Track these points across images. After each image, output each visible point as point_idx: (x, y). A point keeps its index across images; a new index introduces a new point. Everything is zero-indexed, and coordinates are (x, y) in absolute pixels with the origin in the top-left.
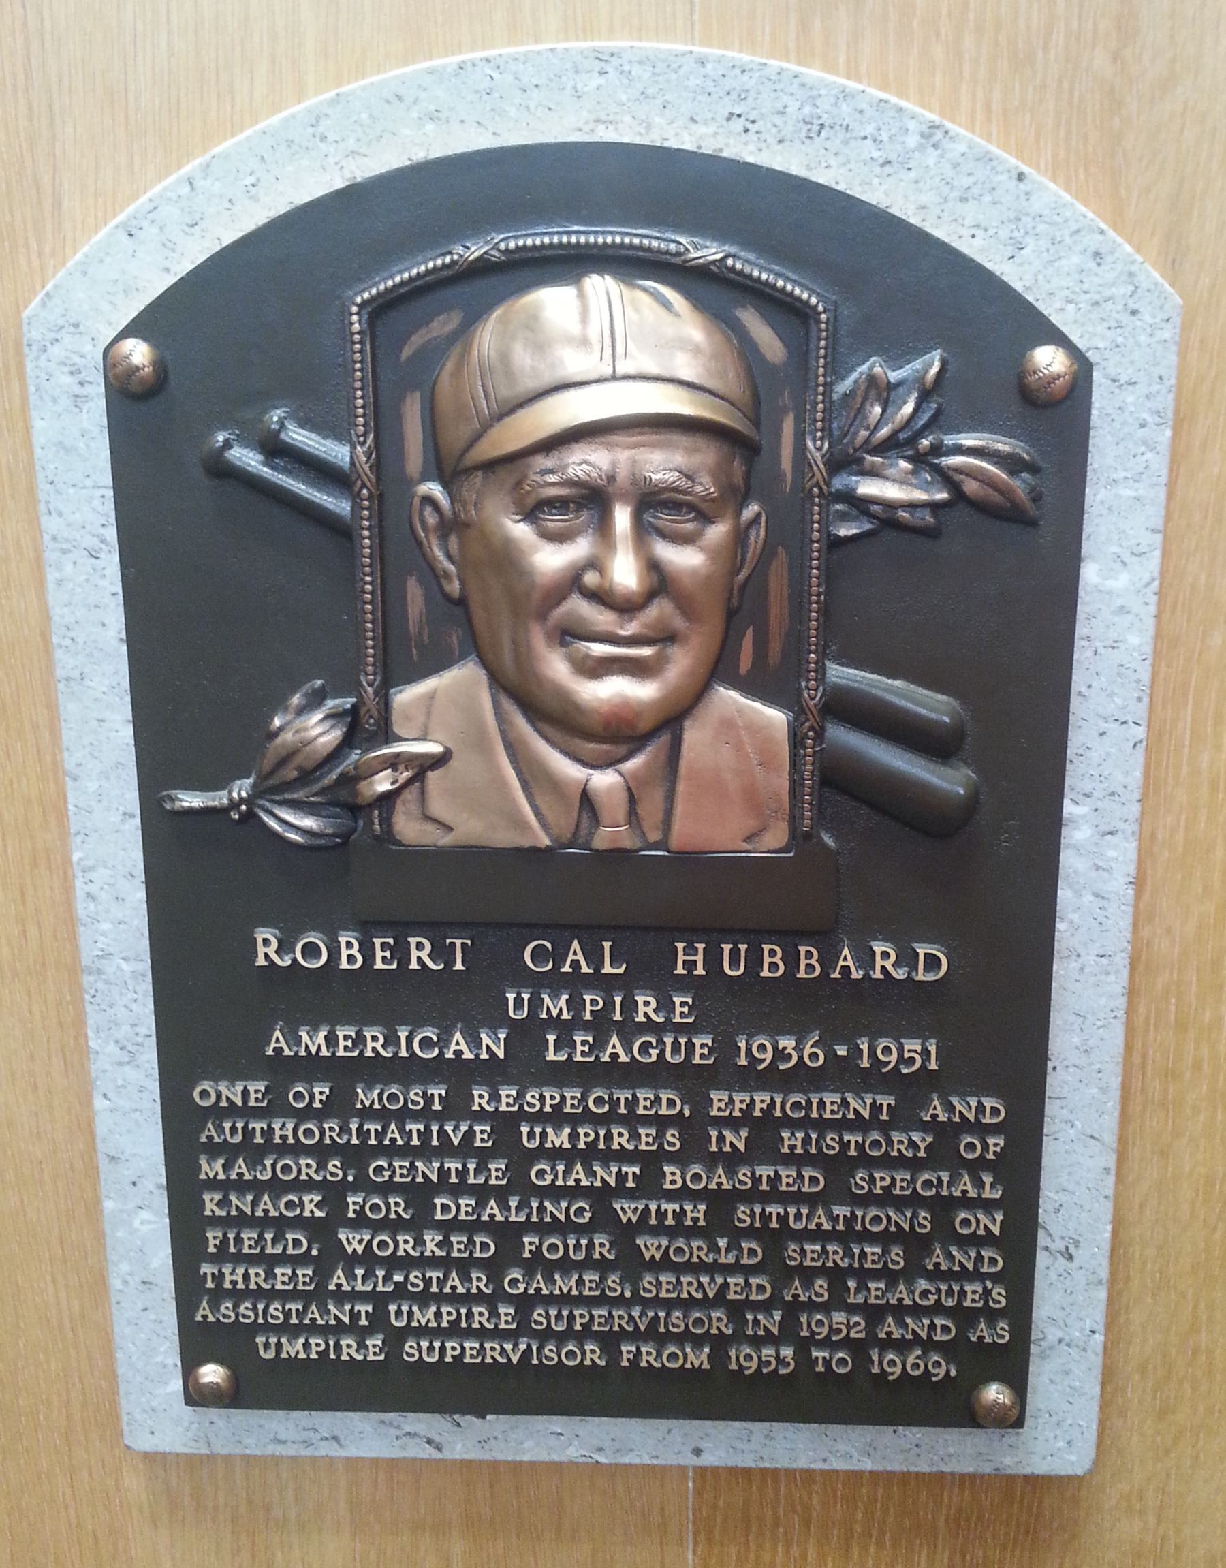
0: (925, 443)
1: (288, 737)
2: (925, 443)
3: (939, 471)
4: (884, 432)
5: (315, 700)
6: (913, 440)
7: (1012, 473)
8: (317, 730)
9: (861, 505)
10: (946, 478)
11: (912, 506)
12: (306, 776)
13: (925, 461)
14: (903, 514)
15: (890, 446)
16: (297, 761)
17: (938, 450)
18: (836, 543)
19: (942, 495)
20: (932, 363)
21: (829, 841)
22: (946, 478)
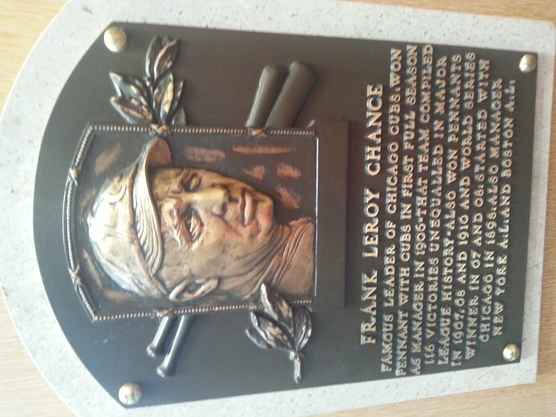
0: (148, 83)
2: (148, 83)
3: (159, 78)
4: (142, 100)
6: (147, 89)
7: (162, 48)
10: (162, 75)
11: (175, 90)
12: (284, 332)
16: (280, 337)
17: (151, 79)
18: (189, 122)
19: (171, 76)
20: (116, 79)
21: (312, 123)
22: (162, 75)
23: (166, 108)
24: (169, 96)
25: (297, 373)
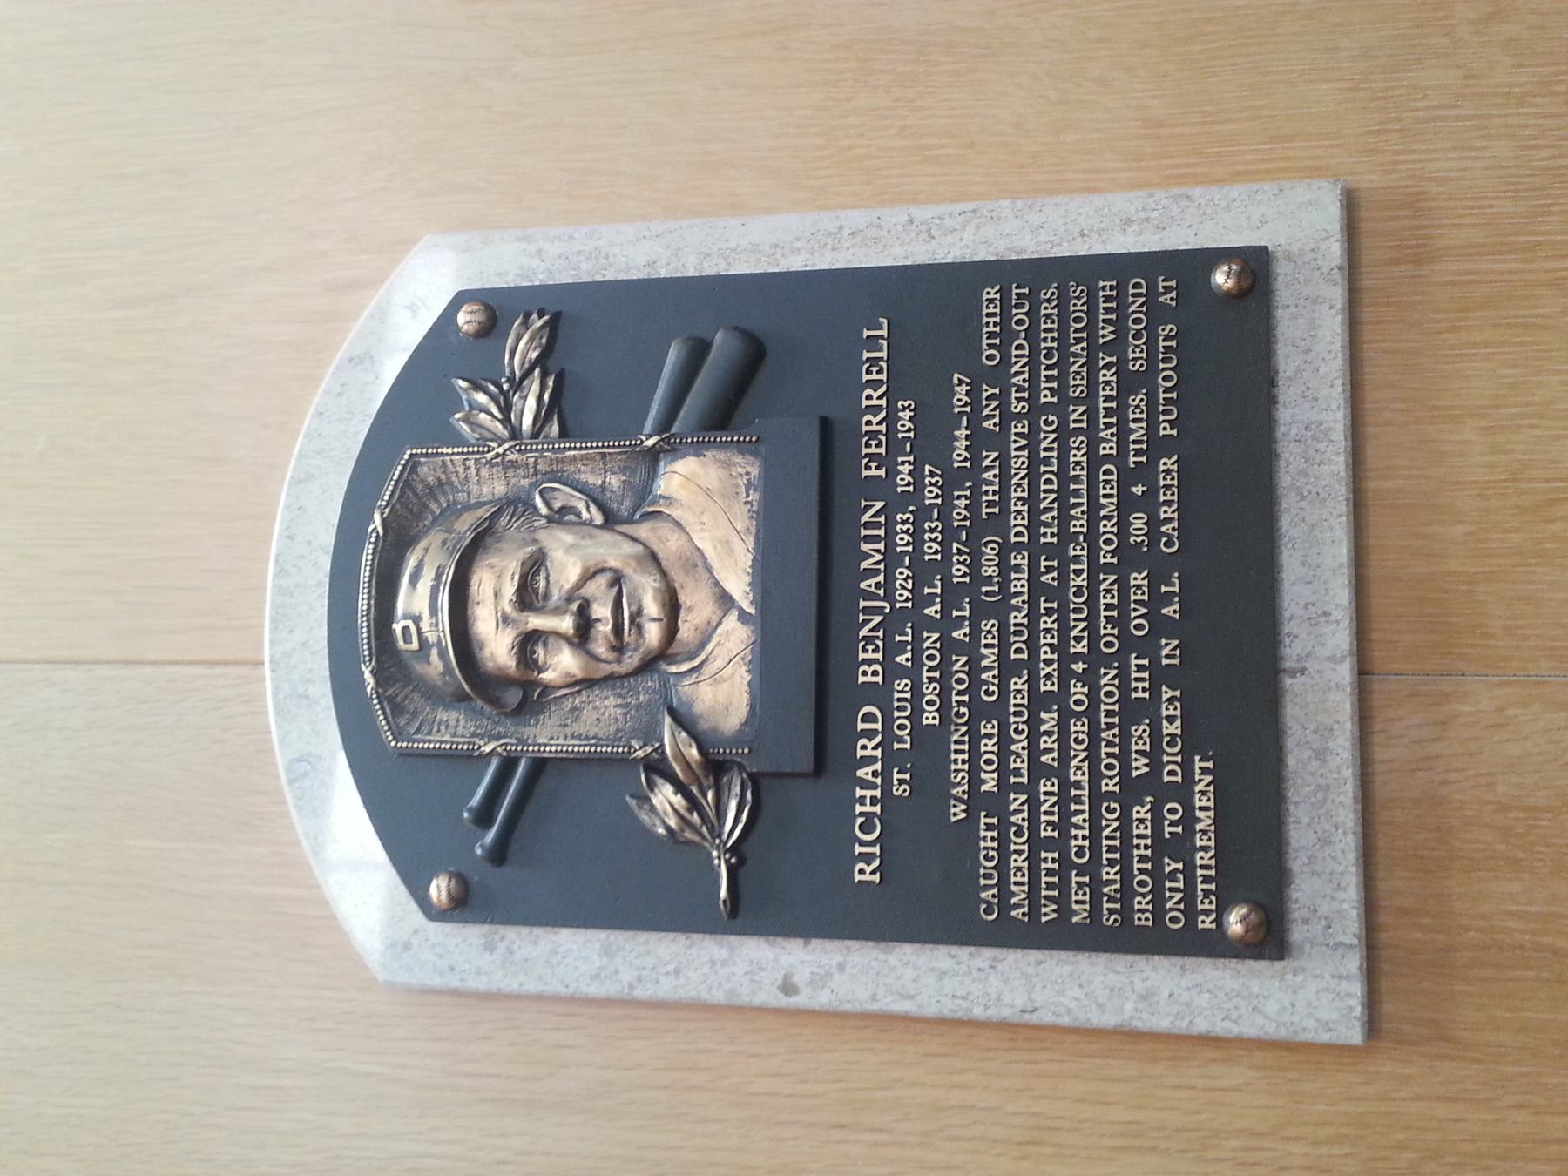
1: (673, 822)
2: (505, 387)
3: (523, 379)
5: (644, 799)
6: (505, 394)
8: (665, 797)
9: (541, 421)
10: (527, 373)
12: (694, 804)
13: (517, 385)
14: (546, 397)
15: (506, 409)
16: (682, 811)
17: (511, 380)
19: (537, 371)
22: (527, 373)
23: (527, 422)
24: (531, 403)
25: (723, 893)
